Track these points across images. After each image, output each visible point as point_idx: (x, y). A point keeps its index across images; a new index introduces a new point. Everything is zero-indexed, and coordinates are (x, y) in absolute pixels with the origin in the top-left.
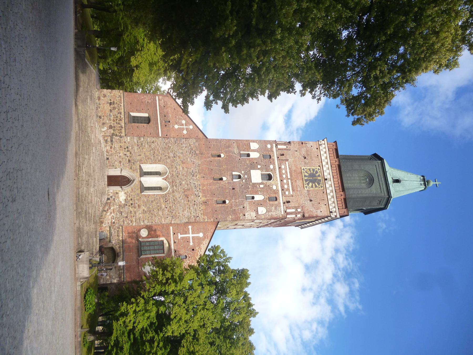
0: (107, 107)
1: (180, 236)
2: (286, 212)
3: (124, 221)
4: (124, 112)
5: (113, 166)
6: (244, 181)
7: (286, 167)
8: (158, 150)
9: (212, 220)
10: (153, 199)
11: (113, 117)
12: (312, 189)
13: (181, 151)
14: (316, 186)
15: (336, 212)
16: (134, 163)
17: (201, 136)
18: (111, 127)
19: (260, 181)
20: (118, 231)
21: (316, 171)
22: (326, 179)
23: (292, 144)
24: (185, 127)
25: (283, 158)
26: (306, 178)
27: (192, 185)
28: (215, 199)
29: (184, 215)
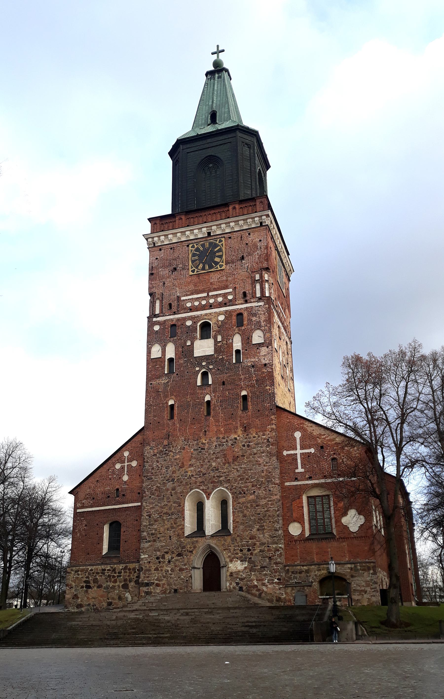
0: (94, 592)
1: (300, 470)
3: (276, 563)
4: (102, 564)
5: (189, 581)
6: (211, 367)
8: (162, 507)
9: (273, 417)
10: (241, 515)
11: (109, 583)
13: (164, 470)
14: (220, 250)
16: (184, 547)
17: (140, 437)
18: (125, 586)
20: (293, 572)
23: (154, 290)
24: (126, 464)
25: (175, 304)
26: (207, 267)
27: (218, 450)
28: (240, 412)
29: (266, 463)
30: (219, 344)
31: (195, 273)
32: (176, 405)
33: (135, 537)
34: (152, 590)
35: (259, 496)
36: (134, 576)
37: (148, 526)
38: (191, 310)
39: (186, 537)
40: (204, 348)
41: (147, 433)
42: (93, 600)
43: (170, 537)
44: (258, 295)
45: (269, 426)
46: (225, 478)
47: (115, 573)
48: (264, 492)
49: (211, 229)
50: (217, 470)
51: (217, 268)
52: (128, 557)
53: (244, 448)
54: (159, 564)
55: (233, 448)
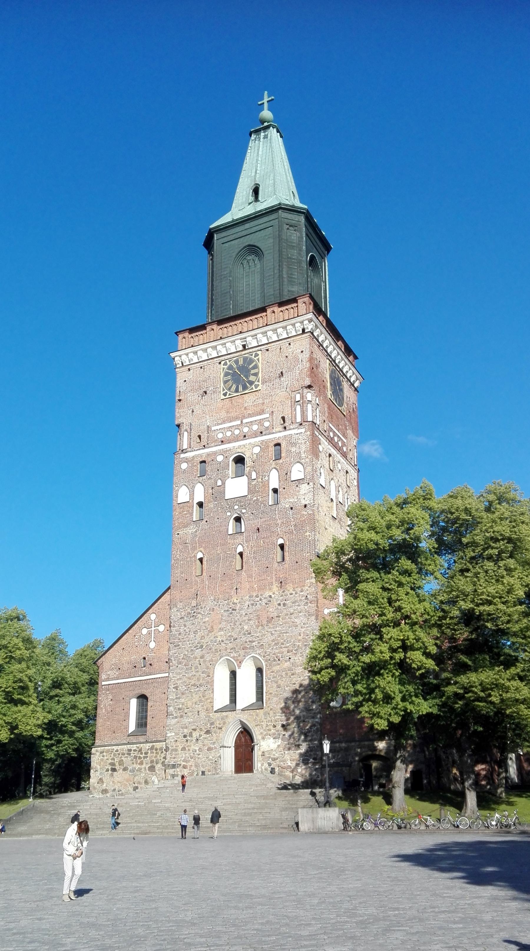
0: (120, 775)
2: (301, 424)
4: (129, 743)
5: (216, 762)
6: (244, 511)
7: (220, 430)
8: (189, 678)
10: (275, 685)
11: (135, 765)
12: (260, 375)
15: (302, 322)
18: (152, 769)
19: (244, 480)
26: (240, 388)
27: (250, 610)
30: (254, 483)
31: (227, 397)
33: (162, 712)
35: (295, 663)
36: (160, 757)
37: (175, 700)
38: (222, 442)
39: (215, 712)
45: (308, 581)
46: (258, 643)
47: (142, 754)
48: (300, 658)
49: (246, 341)
50: (249, 634)
51: (252, 389)
53: (279, 607)
55: (267, 607)
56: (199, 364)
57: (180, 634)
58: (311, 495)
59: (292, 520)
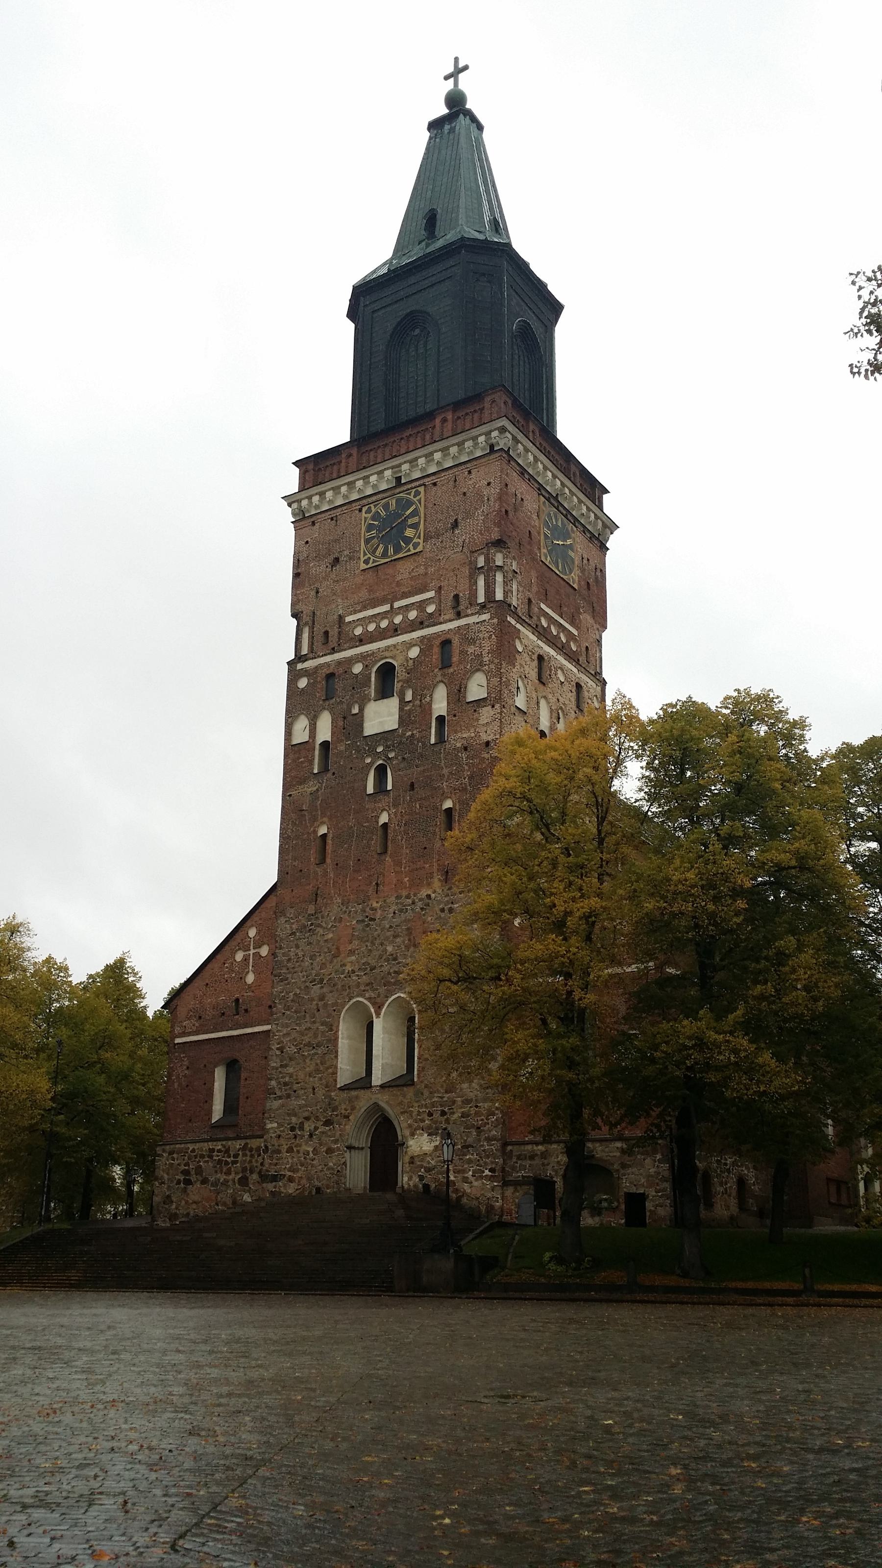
0: (197, 1192)
3: (489, 1139)
4: (212, 1140)
6: (391, 755)
12: (422, 526)
14: (415, 513)
16: (335, 1109)
18: (244, 1181)
20: (519, 1157)
21: (373, 519)
22: (398, 479)
23: (300, 607)
24: (252, 951)
25: (334, 633)
26: (391, 551)
32: (330, 836)
34: (282, 1189)
38: (361, 641)
39: (341, 1089)
40: (381, 716)
41: (280, 891)
42: (194, 1206)
43: (314, 1089)
44: (481, 599)
49: (400, 471)
50: (395, 959)
52: (250, 1125)
53: (443, 915)
54: (293, 1141)
55: (424, 915)
56: (329, 513)
57: (289, 960)
58: (496, 726)
59: (466, 768)
